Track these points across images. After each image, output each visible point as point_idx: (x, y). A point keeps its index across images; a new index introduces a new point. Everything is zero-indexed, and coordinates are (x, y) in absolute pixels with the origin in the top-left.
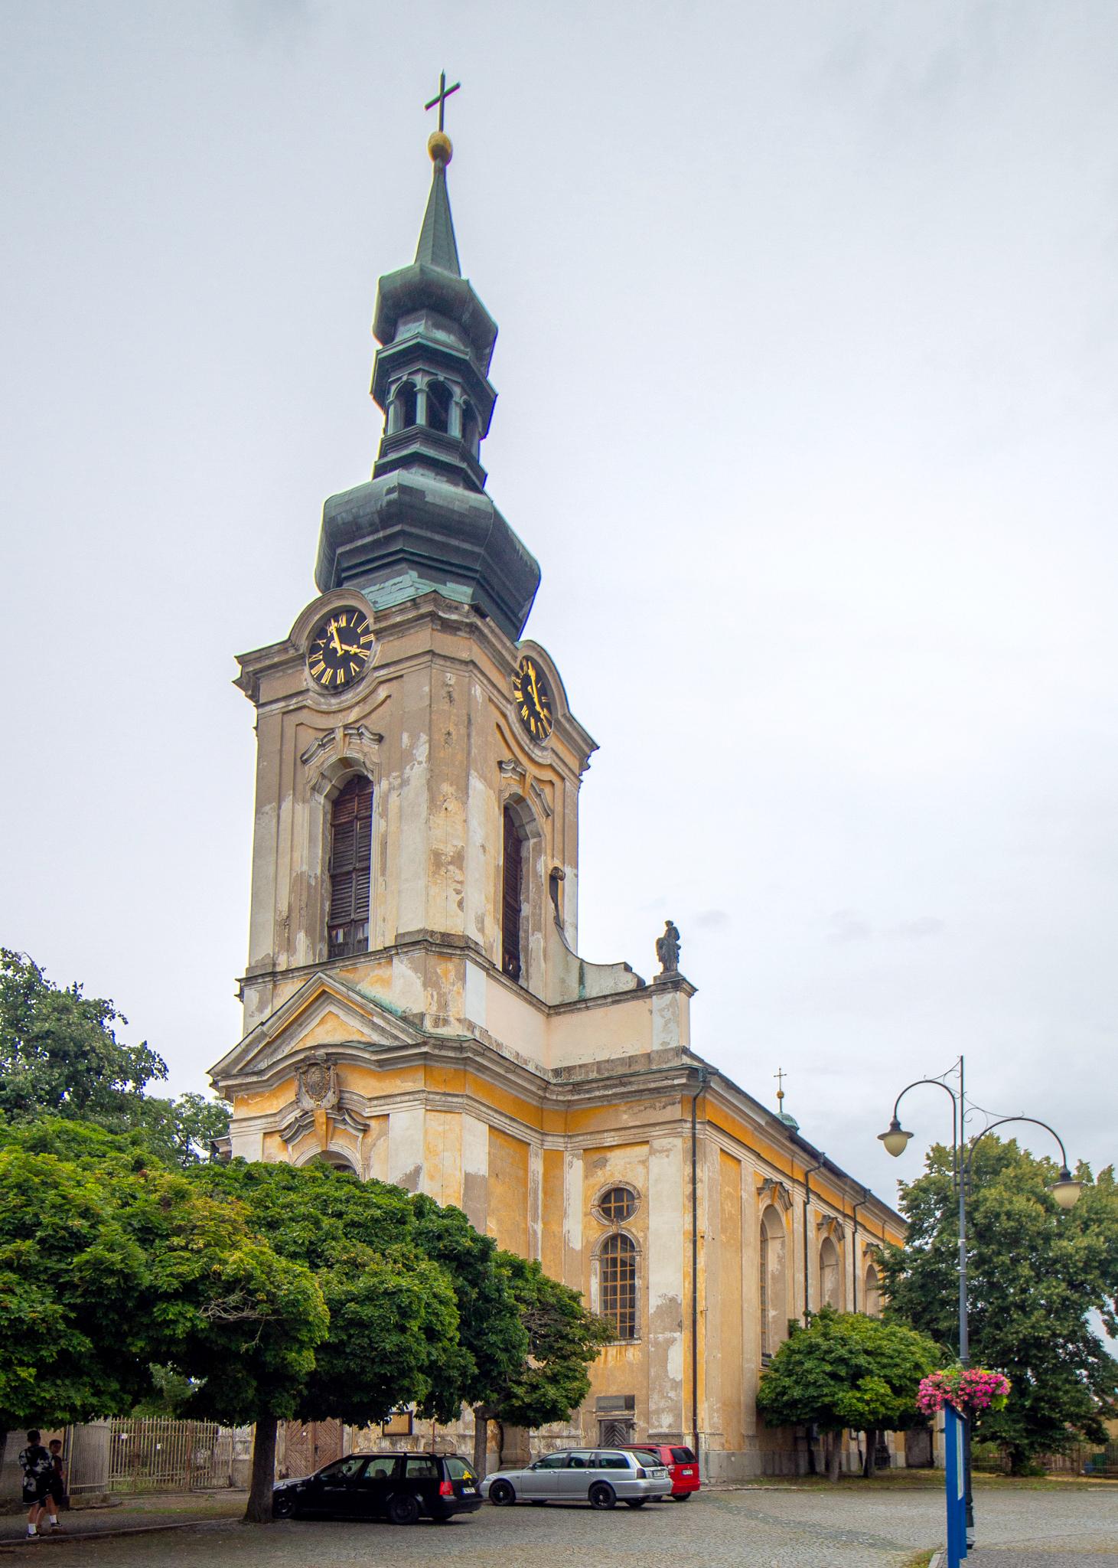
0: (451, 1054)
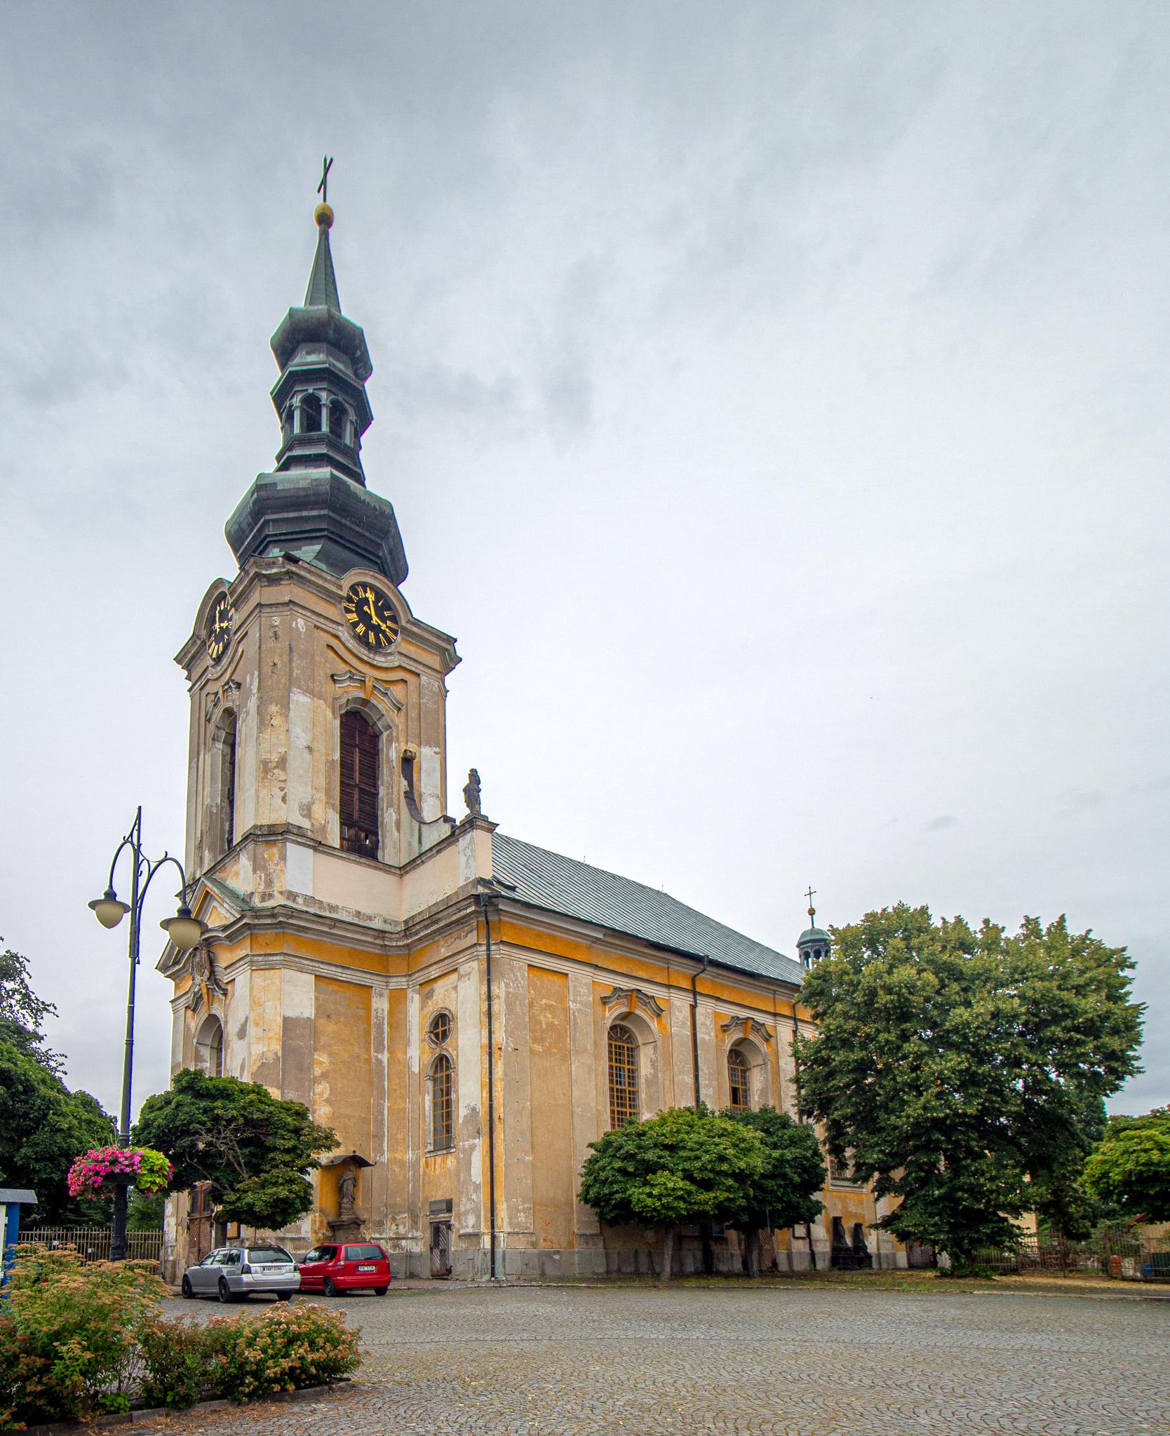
0: (268, 921)
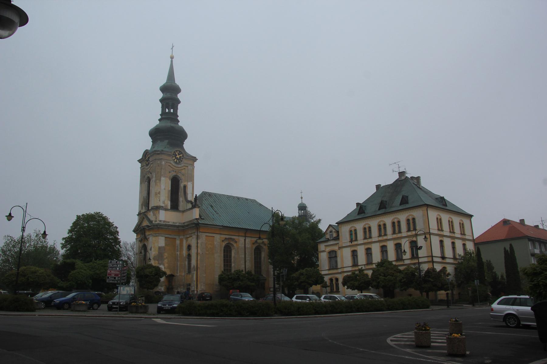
0: (156, 227)
